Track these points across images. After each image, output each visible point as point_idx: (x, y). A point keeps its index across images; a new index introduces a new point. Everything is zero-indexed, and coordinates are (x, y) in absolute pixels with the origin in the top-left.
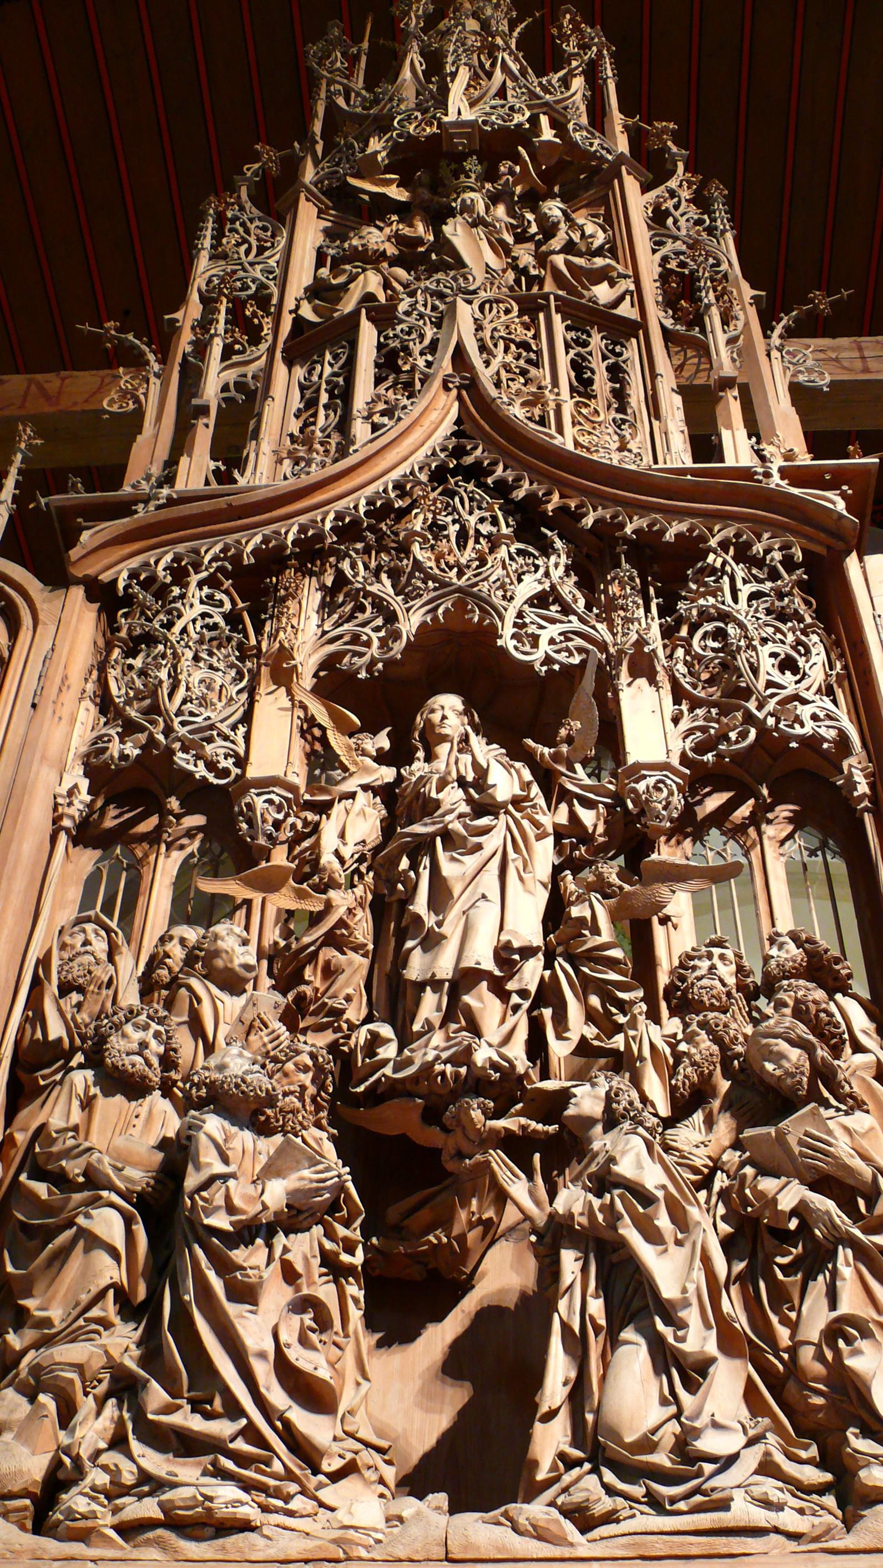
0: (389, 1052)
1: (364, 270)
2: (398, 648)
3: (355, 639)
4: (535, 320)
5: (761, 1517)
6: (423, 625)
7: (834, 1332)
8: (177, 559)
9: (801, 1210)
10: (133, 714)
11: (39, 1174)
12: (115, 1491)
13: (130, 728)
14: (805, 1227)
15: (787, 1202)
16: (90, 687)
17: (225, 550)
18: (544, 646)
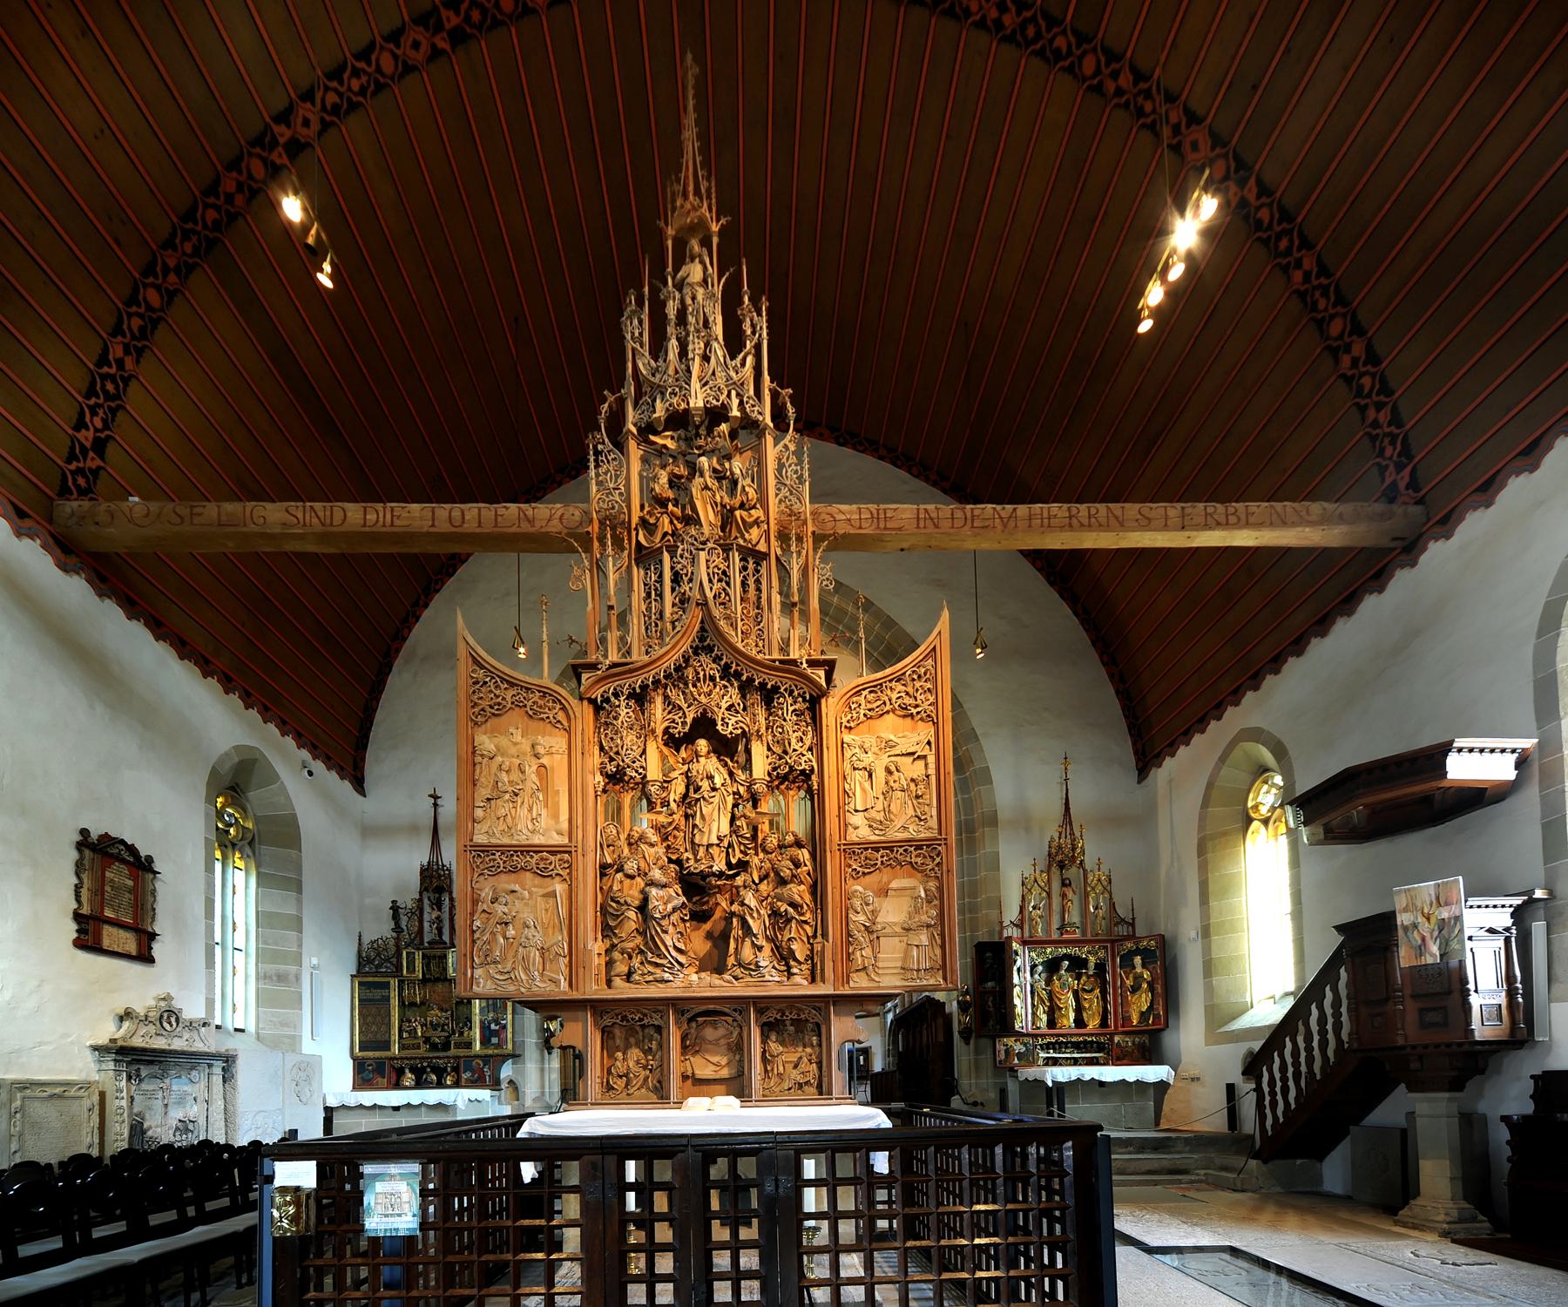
0: (692, 862)
1: (662, 514)
2: (687, 728)
3: (673, 721)
4: (728, 555)
5: (771, 979)
6: (694, 718)
7: (789, 939)
8: (615, 689)
9: (786, 911)
10: (612, 754)
11: (612, 900)
12: (643, 975)
13: (612, 760)
14: (786, 914)
15: (782, 909)
16: (596, 740)
17: (630, 685)
18: (730, 728)
